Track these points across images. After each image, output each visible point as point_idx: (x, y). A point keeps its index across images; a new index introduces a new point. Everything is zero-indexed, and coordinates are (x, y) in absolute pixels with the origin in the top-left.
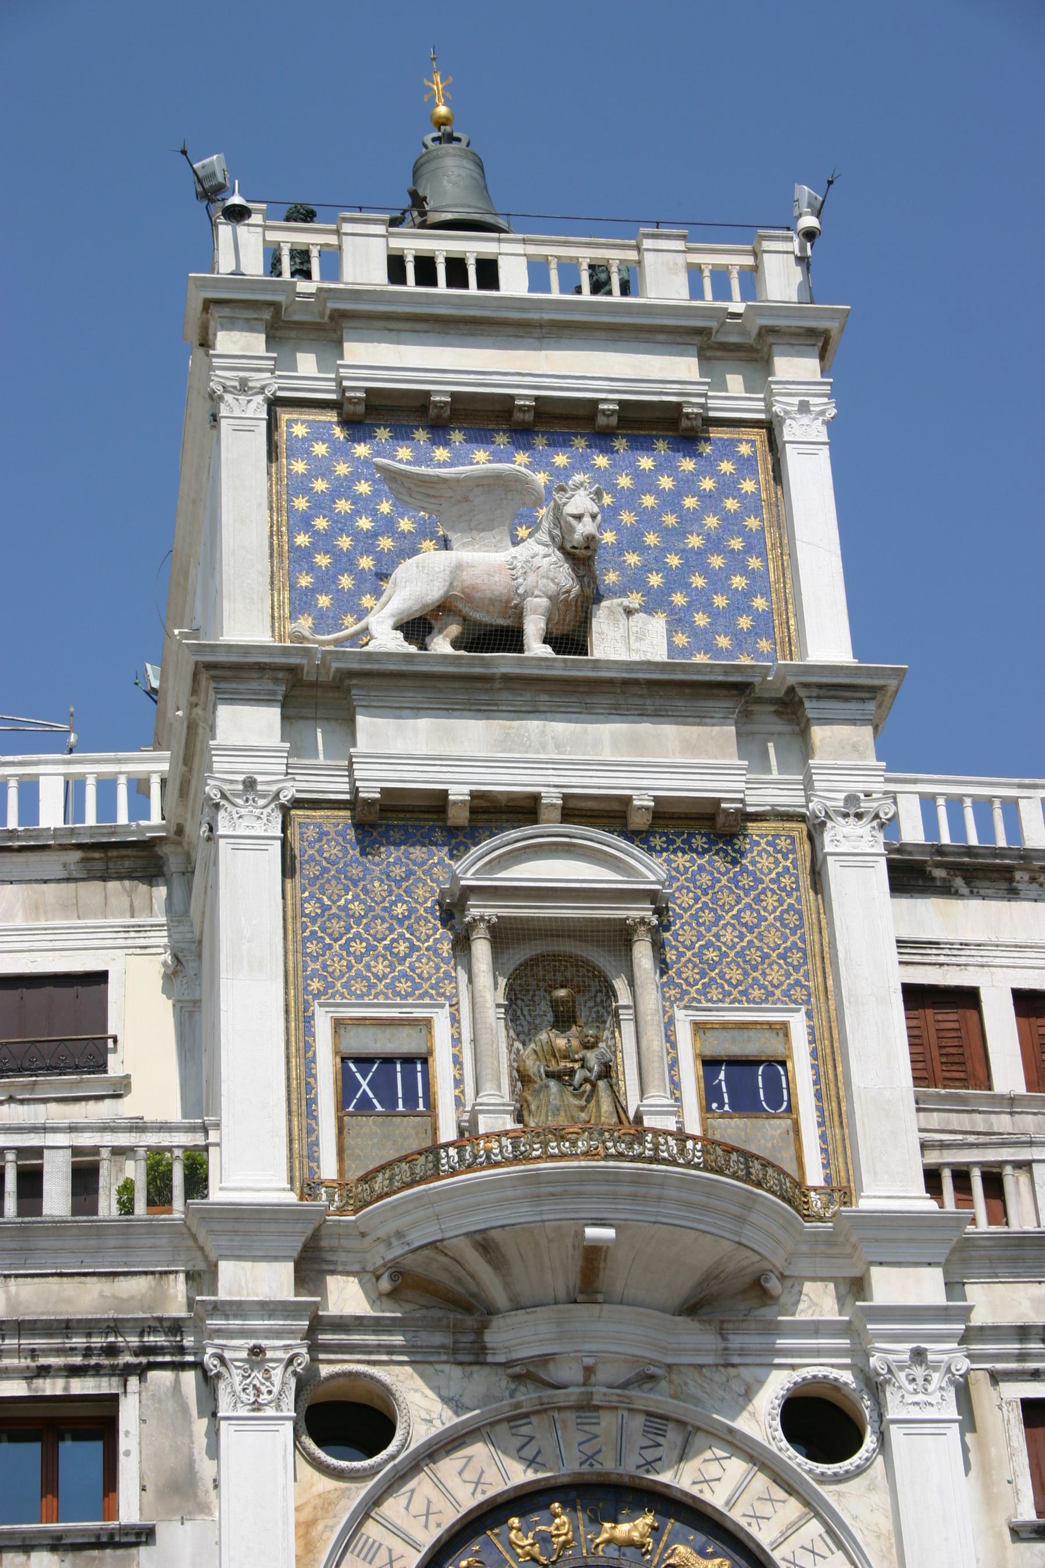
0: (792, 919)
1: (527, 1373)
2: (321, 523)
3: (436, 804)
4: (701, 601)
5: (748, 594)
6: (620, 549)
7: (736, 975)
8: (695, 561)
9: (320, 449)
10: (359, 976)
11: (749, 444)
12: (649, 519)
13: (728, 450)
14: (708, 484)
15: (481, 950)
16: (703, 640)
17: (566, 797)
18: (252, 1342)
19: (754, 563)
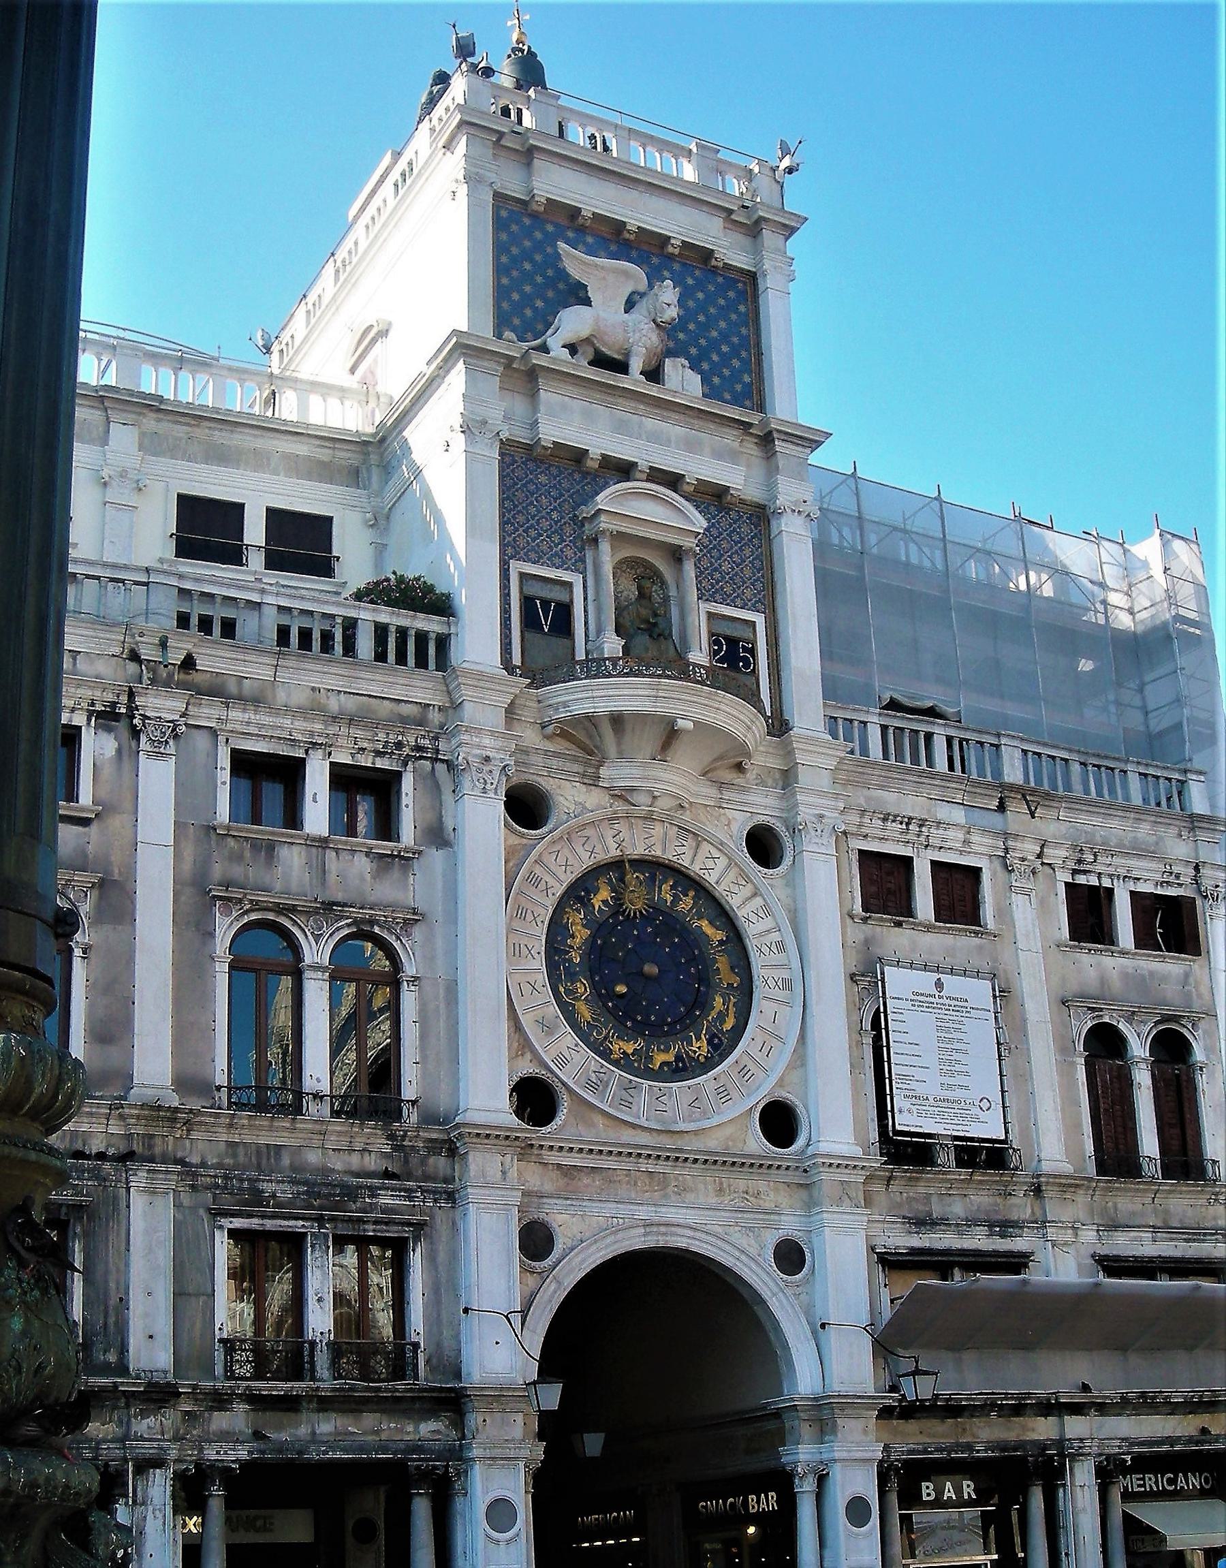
1: (622, 795)
3: (579, 456)
7: (728, 589)
8: (714, 345)
10: (533, 550)
17: (651, 468)
18: (485, 753)
19: (744, 354)
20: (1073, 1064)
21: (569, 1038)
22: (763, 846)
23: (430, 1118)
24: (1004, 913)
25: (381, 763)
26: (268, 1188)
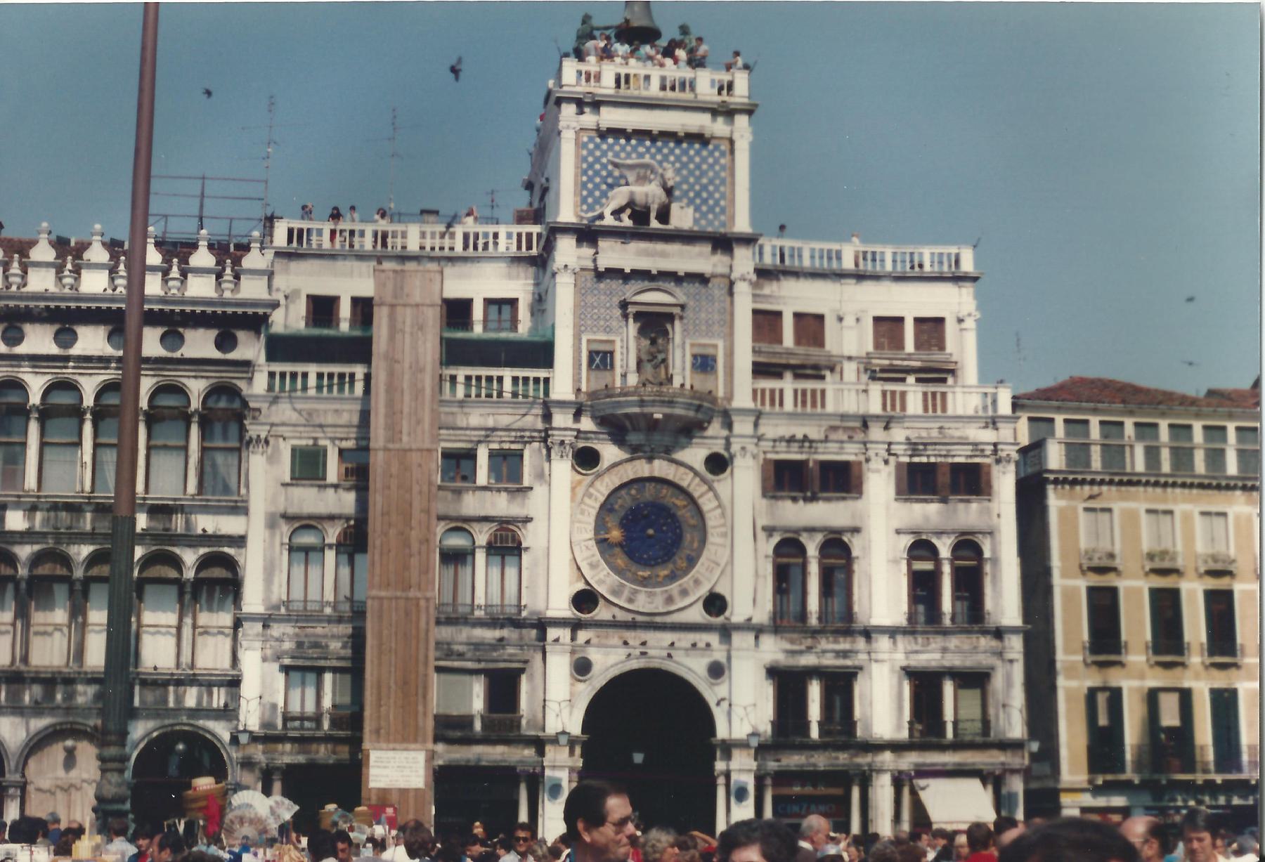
2: (590, 173)
4: (705, 201)
8: (704, 188)
11: (724, 147)
12: (691, 173)
13: (717, 148)
15: (631, 320)
16: (704, 215)
21: (605, 570)
23: (532, 613)
25: (514, 446)
26: (456, 647)
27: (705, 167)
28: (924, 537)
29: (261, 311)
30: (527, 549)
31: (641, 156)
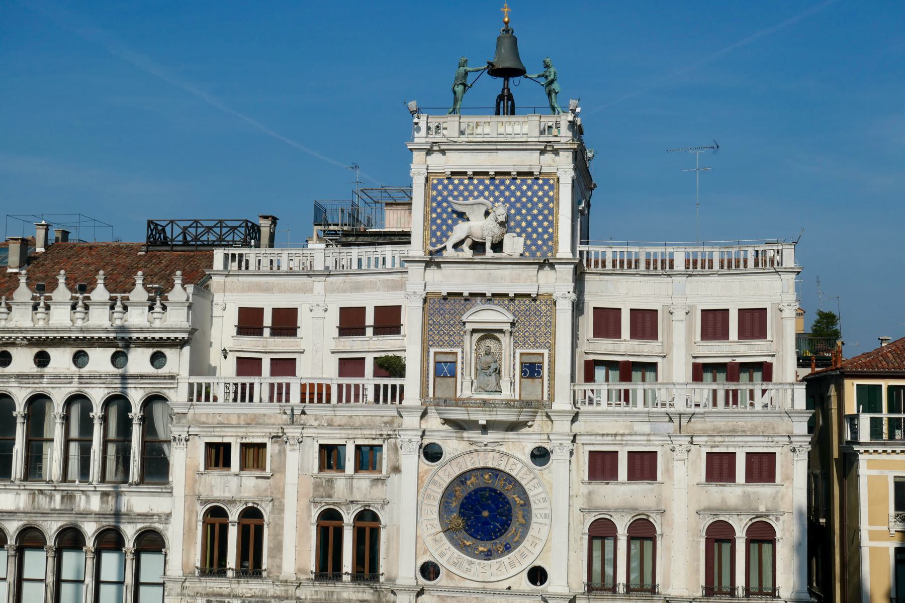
0: (548, 324)
2: (439, 210)
3: (461, 294)
5: (548, 228)
6: (515, 215)
8: (535, 217)
9: (440, 187)
12: (524, 205)
14: (540, 193)
15: (467, 338)
16: (534, 242)
20: (698, 543)
22: (541, 456)
24: (668, 471)
27: (535, 199)
28: (722, 518)
29: (180, 336)
30: (385, 526)
31: (481, 194)
